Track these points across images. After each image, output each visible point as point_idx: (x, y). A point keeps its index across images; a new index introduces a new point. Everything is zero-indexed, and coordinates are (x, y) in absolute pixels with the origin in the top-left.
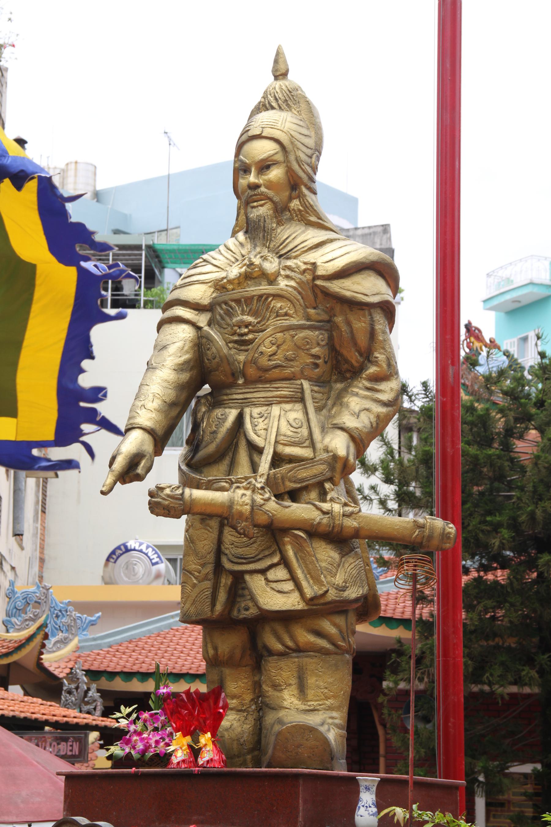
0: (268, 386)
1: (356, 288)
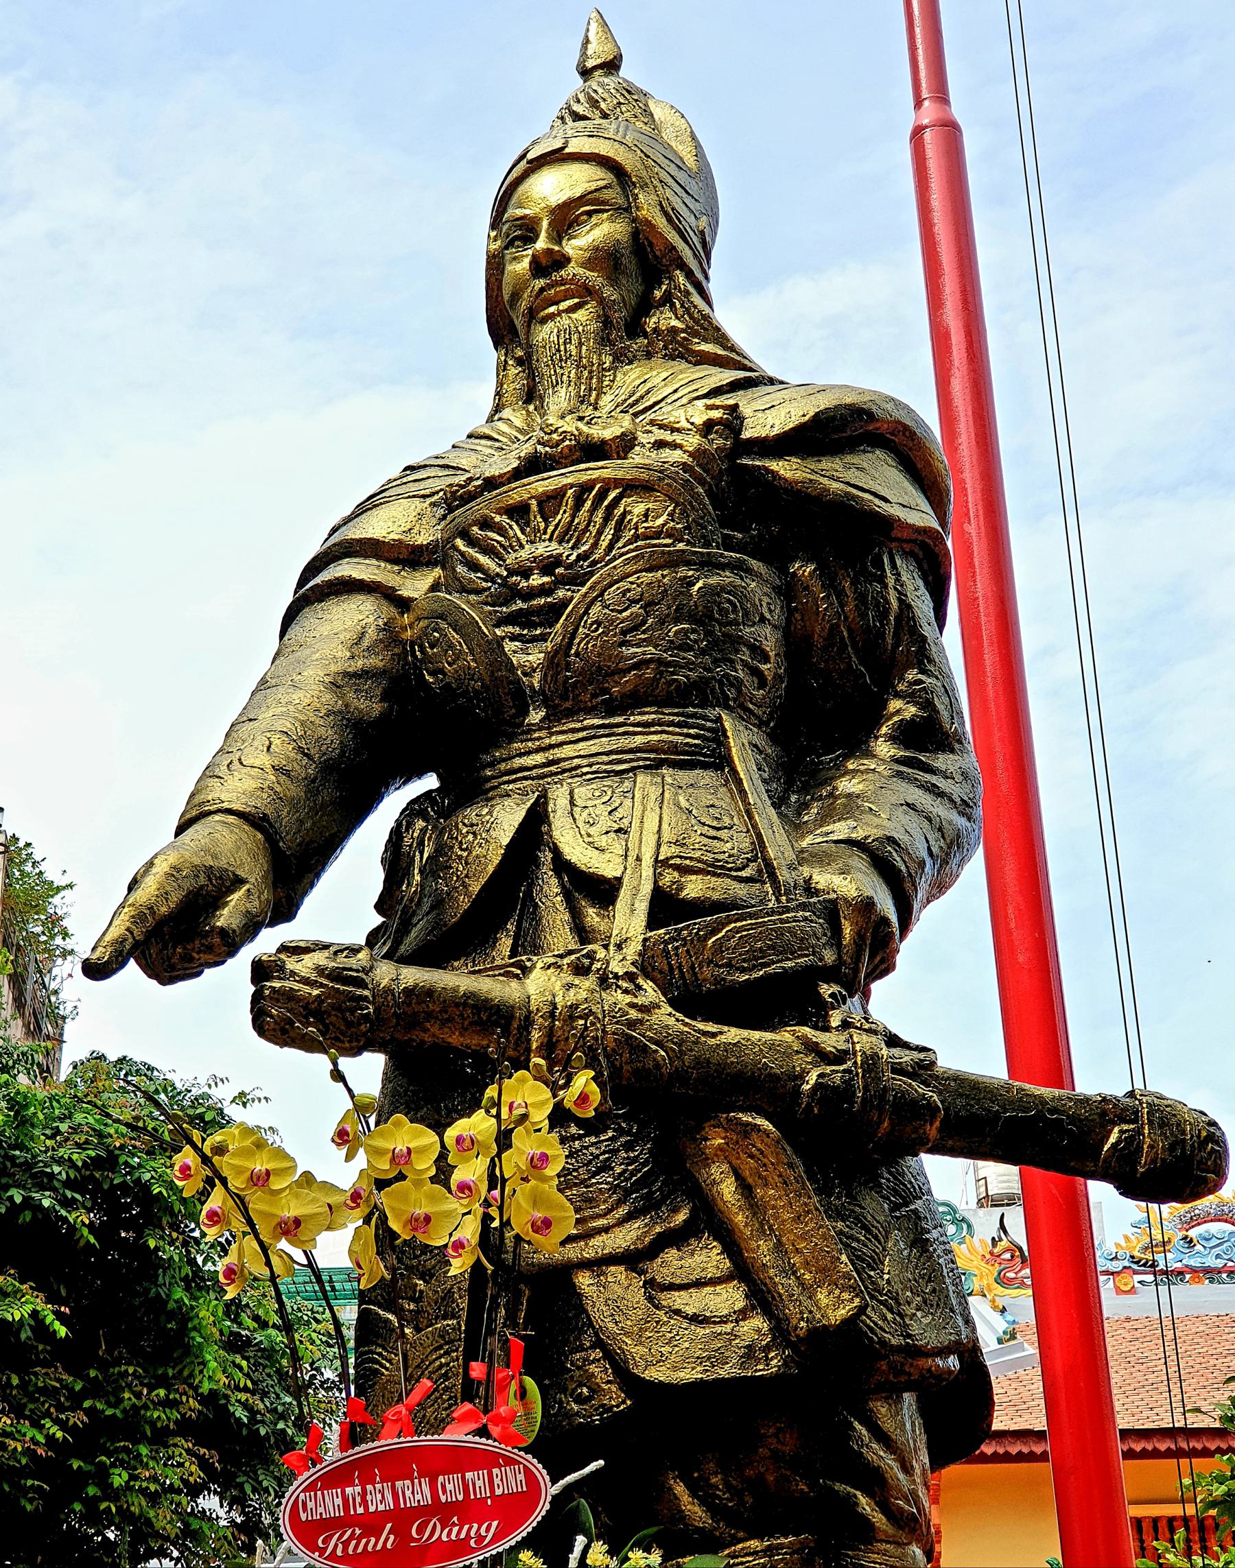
0: (620, 719)
1: (852, 476)
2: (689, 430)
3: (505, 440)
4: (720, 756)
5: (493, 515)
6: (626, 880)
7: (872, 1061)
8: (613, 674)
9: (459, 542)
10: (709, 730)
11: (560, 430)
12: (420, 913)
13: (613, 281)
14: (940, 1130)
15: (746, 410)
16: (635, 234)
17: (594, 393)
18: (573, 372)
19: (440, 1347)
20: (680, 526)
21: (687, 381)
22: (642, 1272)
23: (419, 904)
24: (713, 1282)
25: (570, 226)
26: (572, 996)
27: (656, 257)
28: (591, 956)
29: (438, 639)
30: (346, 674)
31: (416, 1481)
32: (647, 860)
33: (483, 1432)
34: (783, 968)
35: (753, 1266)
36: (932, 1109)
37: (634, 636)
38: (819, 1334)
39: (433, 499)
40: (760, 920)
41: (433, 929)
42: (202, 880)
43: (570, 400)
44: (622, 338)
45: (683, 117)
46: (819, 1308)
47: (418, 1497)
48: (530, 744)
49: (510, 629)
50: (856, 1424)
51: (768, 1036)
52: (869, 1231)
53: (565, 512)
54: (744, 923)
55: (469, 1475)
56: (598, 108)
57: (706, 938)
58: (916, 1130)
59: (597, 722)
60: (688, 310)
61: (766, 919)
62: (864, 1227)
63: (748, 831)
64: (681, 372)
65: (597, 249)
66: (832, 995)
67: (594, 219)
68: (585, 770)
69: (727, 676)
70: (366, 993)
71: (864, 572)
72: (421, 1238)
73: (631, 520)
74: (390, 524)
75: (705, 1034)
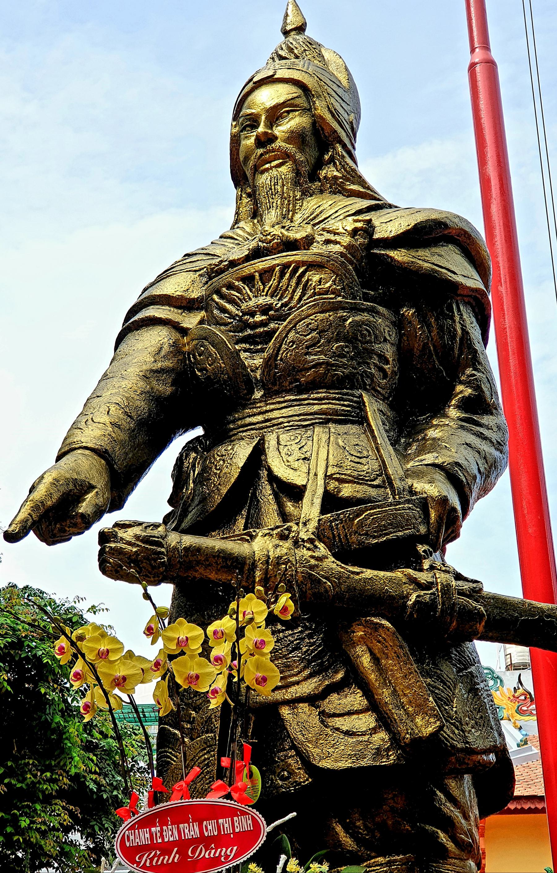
0: (305, 396)
1: (436, 260)
2: (344, 234)
3: (240, 239)
4: (362, 417)
5: (234, 281)
6: (309, 487)
7: (446, 588)
8: (301, 370)
9: (215, 297)
10: (355, 402)
11: (272, 234)
12: (194, 505)
13: (302, 150)
14: (485, 627)
15: (376, 222)
16: (314, 124)
17: (291, 213)
18: (279, 201)
19: (204, 749)
20: (339, 287)
21: (343, 206)
22: (317, 707)
23: (192, 500)
24: (358, 712)
25: (277, 119)
26: (278, 552)
27: (325, 136)
28: (289, 529)
29: (203, 351)
30: (152, 371)
31: (191, 824)
32: (321, 475)
33: (228, 797)
34: (397, 536)
35: (380, 703)
36: (480, 615)
37: (313, 349)
38: (417, 742)
39: (200, 273)
40: (384, 509)
41: (201, 514)
42: (71, 486)
43: (277, 217)
44: (306, 182)
45: (341, 58)
46: (417, 727)
47: (192, 833)
48: (255, 410)
49: (244, 345)
50: (438, 792)
51: (388, 574)
52: (445, 684)
53: (274, 280)
54: (375, 511)
55: (221, 821)
56: (293, 52)
57: (354, 519)
58: (471, 627)
59: (292, 397)
60: (343, 166)
61: (387, 509)
62: (442, 681)
63: (377, 459)
64: (340, 201)
65: (292, 132)
66: (425, 551)
67: (291, 115)
68: (286, 424)
69: (365, 372)
70: (163, 550)
71: (442, 313)
72: (194, 688)
73: (312, 284)
74: (176, 286)
75: (353, 573)
